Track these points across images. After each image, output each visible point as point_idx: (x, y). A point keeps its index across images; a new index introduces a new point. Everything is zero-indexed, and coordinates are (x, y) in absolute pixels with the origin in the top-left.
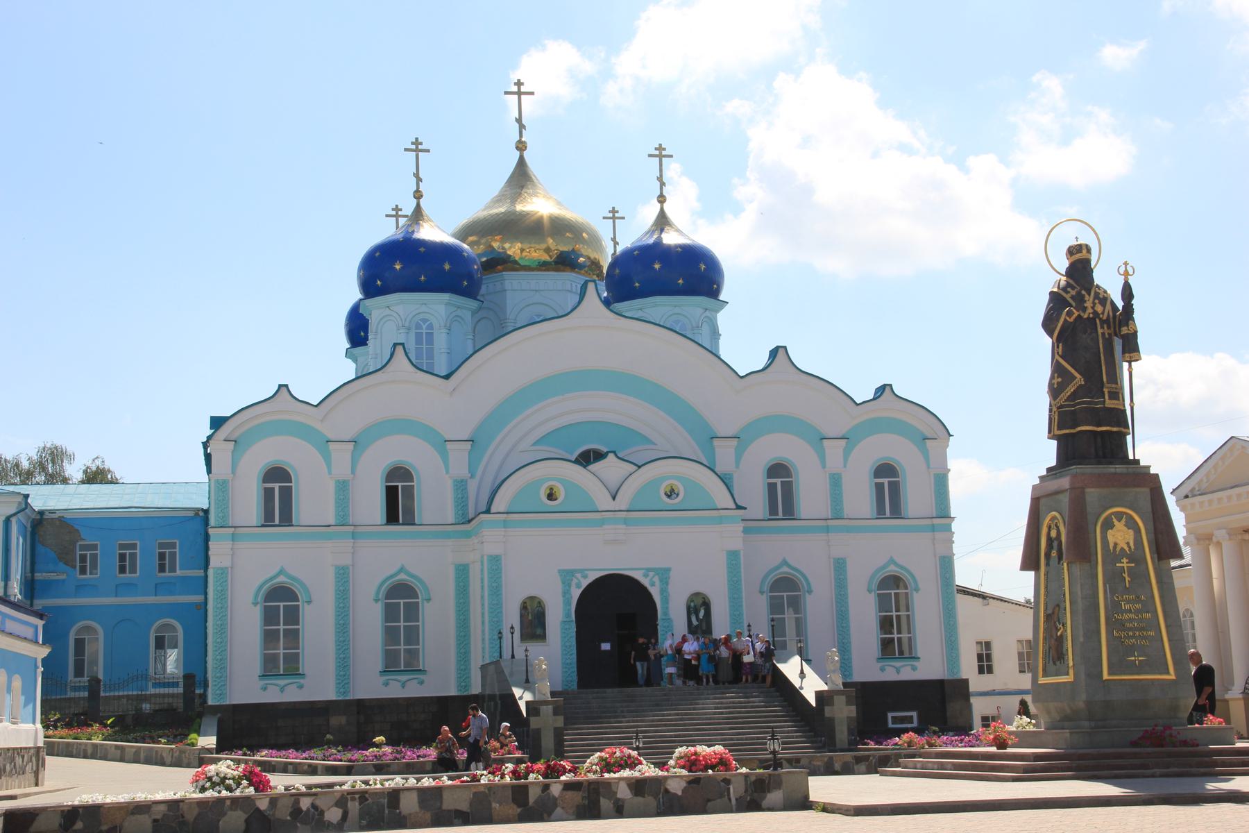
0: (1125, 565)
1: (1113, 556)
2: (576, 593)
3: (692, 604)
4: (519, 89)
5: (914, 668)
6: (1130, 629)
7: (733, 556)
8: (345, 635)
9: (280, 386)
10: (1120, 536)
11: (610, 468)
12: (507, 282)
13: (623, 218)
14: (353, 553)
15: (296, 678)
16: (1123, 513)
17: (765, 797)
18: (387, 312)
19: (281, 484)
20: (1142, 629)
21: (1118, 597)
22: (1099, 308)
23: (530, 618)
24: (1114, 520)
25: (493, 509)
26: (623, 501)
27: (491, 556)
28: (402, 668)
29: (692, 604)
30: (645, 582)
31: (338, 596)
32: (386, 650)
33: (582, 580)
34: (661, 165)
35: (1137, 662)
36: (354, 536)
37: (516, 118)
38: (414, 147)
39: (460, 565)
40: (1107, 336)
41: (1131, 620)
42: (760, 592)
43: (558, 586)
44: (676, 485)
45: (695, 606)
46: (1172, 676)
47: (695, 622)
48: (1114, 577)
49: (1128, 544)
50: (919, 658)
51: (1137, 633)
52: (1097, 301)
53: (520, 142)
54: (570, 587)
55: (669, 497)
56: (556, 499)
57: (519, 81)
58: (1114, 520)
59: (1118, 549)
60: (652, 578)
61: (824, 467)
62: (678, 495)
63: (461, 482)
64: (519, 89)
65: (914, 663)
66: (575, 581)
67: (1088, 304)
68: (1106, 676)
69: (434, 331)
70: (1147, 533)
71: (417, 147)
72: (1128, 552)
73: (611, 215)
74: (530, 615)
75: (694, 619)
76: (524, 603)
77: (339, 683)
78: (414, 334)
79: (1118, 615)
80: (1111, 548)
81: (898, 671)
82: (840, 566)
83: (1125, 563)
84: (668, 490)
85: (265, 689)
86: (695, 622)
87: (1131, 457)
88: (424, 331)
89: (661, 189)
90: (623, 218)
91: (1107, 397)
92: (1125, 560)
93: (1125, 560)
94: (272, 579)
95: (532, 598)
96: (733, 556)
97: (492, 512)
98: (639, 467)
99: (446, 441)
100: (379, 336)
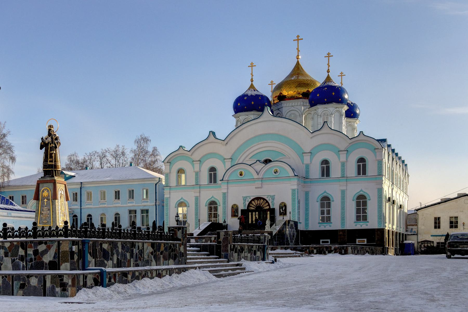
1: (44, 198)
3: (281, 206)
4: (298, 38)
7: (293, 190)
10: (45, 194)
12: (283, 104)
14: (170, 194)
16: (47, 189)
18: (238, 119)
19: (363, 163)
29: (281, 206)
33: (249, 199)
34: (329, 60)
42: (317, 201)
43: (242, 201)
45: (282, 206)
47: (282, 211)
49: (47, 196)
54: (245, 201)
55: (275, 173)
61: (339, 160)
64: (298, 38)
65: (331, 224)
66: (247, 200)
75: (281, 210)
76: (233, 206)
82: (343, 193)
83: (46, 200)
84: (275, 171)
90: (345, 75)
92: (46, 200)
93: (46, 200)
94: (179, 200)
95: (235, 205)
96: (293, 190)
97: (223, 180)
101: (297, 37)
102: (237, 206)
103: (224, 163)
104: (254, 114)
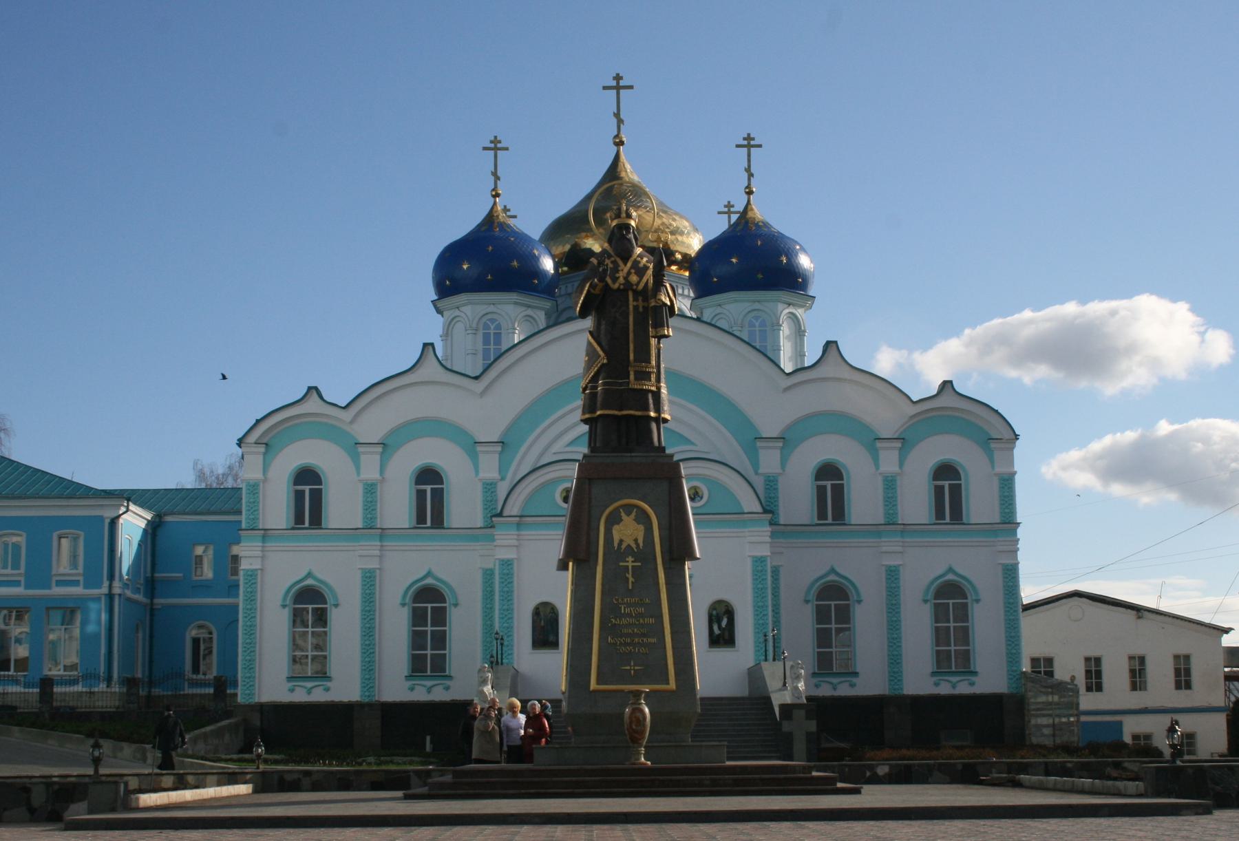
0: (630, 565)
1: (615, 554)
3: (714, 613)
4: (618, 83)
6: (628, 635)
7: (759, 561)
8: (371, 638)
9: (310, 389)
10: (628, 532)
15: (323, 681)
17: (67, 808)
18: (457, 313)
20: (644, 635)
21: (617, 600)
22: (634, 278)
24: (623, 514)
25: (505, 514)
27: (503, 560)
29: (714, 613)
32: (413, 655)
34: (749, 155)
35: (632, 672)
36: (382, 537)
38: (492, 145)
39: (487, 570)
40: (641, 309)
41: (629, 625)
44: (699, 488)
45: (717, 614)
46: (672, 685)
48: (614, 578)
49: (636, 540)
50: (858, 673)
51: (636, 640)
52: (633, 271)
53: (617, 136)
57: (618, 75)
58: (623, 514)
59: (623, 547)
62: (702, 498)
63: (491, 485)
64: (618, 83)
67: (621, 275)
68: (593, 685)
69: (502, 331)
70: (660, 529)
71: (495, 146)
72: (636, 550)
73: (726, 210)
74: (542, 622)
75: (715, 628)
77: (364, 687)
78: (482, 334)
79: (616, 620)
80: (616, 545)
81: (954, 687)
82: (893, 574)
83: (630, 562)
85: (292, 691)
87: (656, 443)
88: (492, 332)
89: (749, 180)
91: (632, 377)
92: (630, 559)
96: (759, 561)
97: (504, 515)
99: (476, 443)
100: (450, 338)
101: (614, 78)
103: (474, 456)
104: (516, 303)
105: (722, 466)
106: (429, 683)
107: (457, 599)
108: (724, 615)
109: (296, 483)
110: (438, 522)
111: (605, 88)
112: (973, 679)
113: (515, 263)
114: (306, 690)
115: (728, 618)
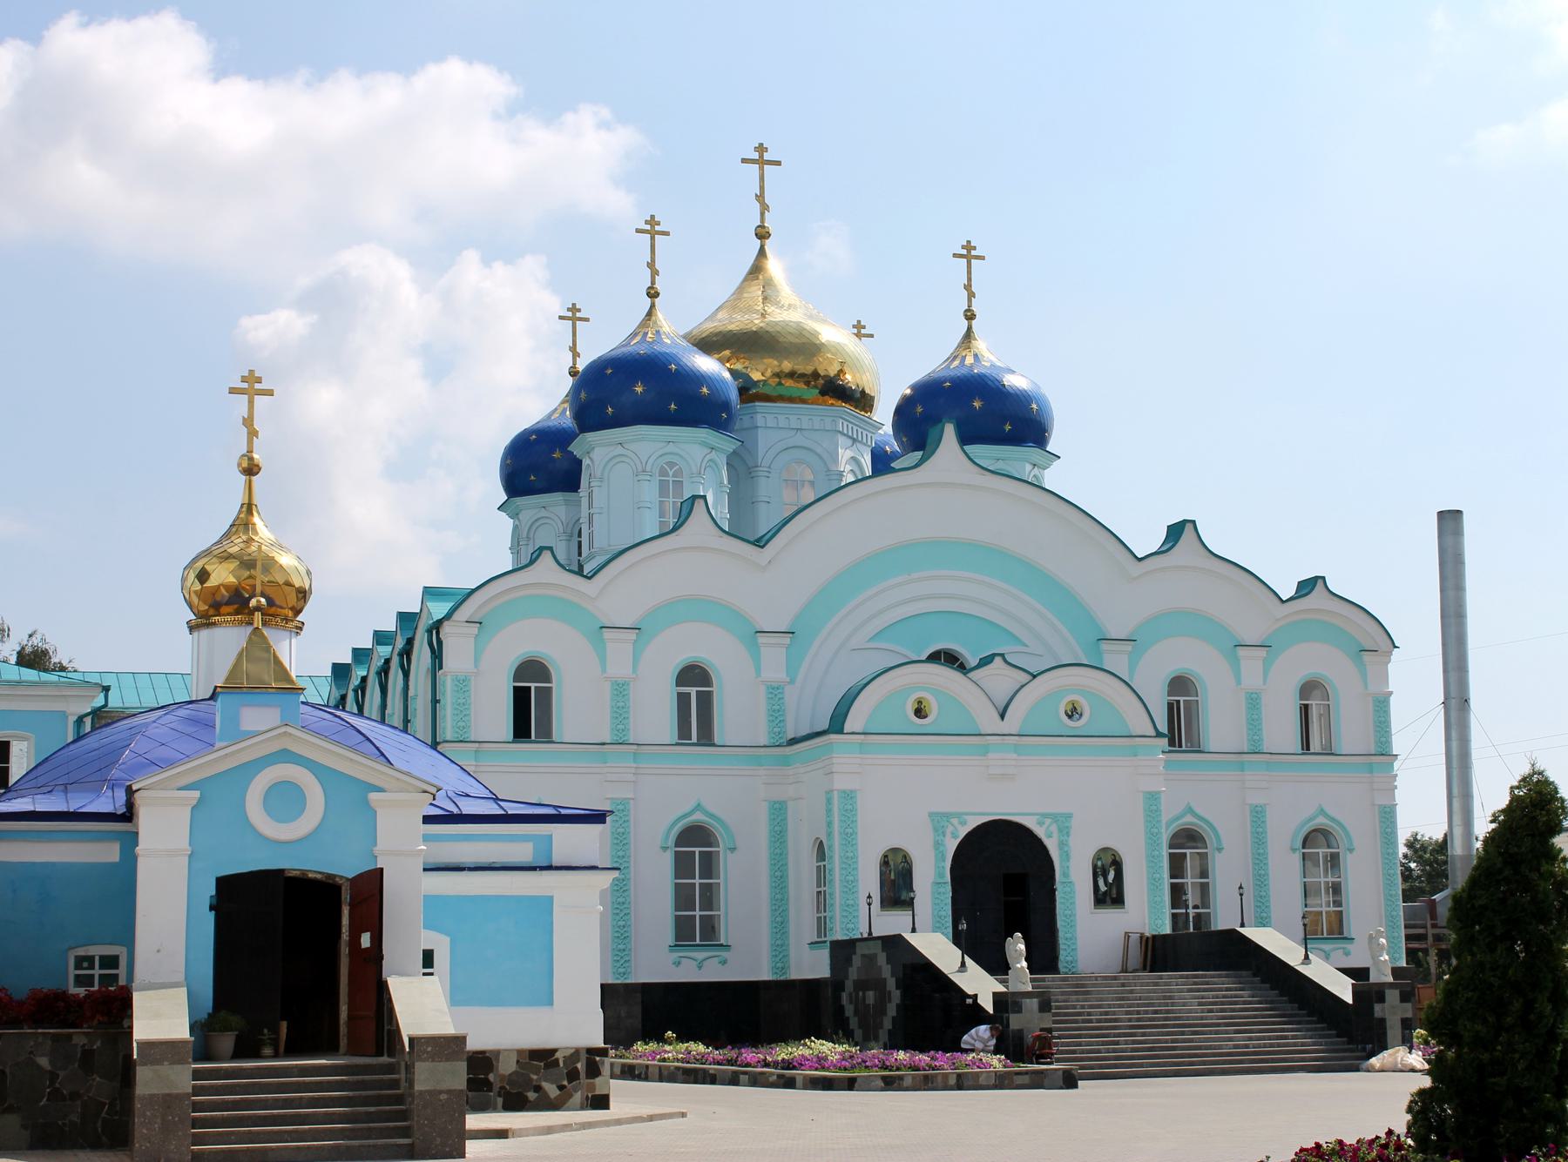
2: (951, 846)
3: (1099, 863)
4: (761, 156)
5: (1347, 954)
11: (998, 679)
12: (759, 416)
13: (872, 336)
18: (620, 450)
23: (893, 877)
26: (1013, 722)
27: (844, 792)
28: (698, 942)
29: (1099, 863)
30: (1040, 832)
31: (773, 839)
33: (959, 827)
37: (756, 195)
44: (1077, 702)
45: (1103, 865)
47: (1103, 888)
53: (762, 226)
55: (1070, 717)
56: (925, 717)
57: (761, 145)
60: (1048, 827)
61: (1239, 682)
62: (1081, 715)
63: (778, 688)
64: (761, 156)
66: (951, 828)
74: (892, 874)
75: (1101, 882)
76: (885, 856)
82: (1258, 815)
86: (1103, 888)
88: (671, 479)
89: (970, 301)
95: (895, 850)
97: (845, 732)
98: (1034, 677)
102: (906, 859)
105: (1108, 675)
106: (700, 955)
107: (1352, 844)
108: (1110, 867)
109: (516, 678)
110: (706, 738)
111: (744, 161)
112: (1349, 946)
113: (705, 390)
114: (695, 963)
115: (1116, 871)
